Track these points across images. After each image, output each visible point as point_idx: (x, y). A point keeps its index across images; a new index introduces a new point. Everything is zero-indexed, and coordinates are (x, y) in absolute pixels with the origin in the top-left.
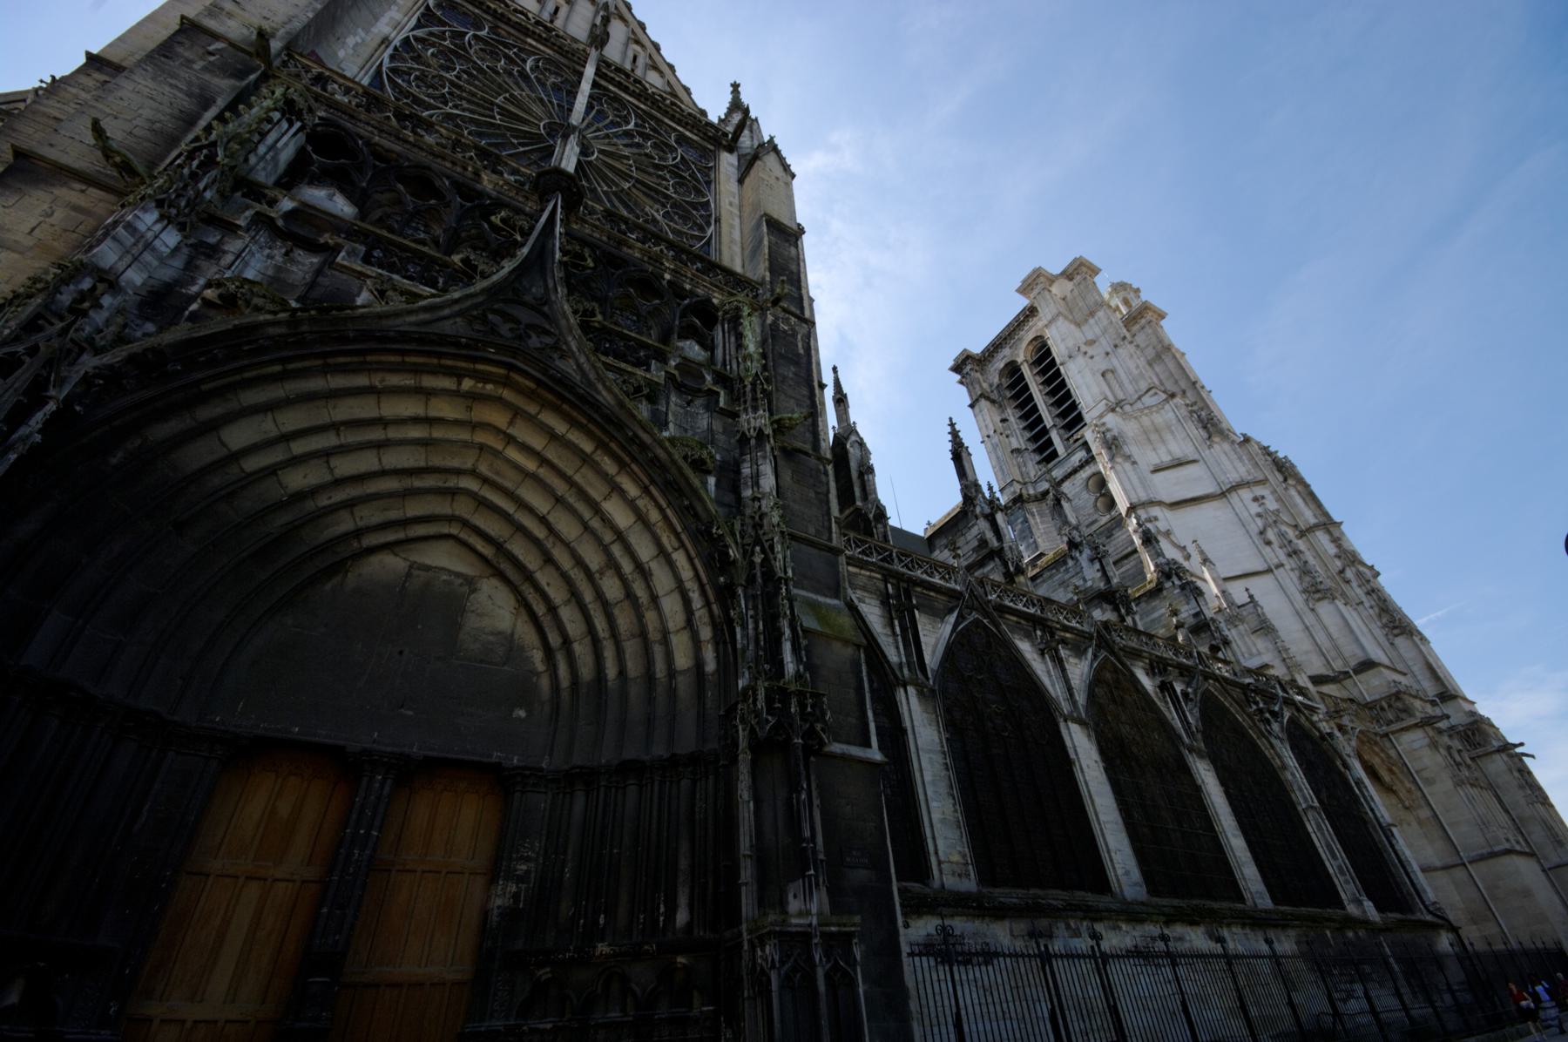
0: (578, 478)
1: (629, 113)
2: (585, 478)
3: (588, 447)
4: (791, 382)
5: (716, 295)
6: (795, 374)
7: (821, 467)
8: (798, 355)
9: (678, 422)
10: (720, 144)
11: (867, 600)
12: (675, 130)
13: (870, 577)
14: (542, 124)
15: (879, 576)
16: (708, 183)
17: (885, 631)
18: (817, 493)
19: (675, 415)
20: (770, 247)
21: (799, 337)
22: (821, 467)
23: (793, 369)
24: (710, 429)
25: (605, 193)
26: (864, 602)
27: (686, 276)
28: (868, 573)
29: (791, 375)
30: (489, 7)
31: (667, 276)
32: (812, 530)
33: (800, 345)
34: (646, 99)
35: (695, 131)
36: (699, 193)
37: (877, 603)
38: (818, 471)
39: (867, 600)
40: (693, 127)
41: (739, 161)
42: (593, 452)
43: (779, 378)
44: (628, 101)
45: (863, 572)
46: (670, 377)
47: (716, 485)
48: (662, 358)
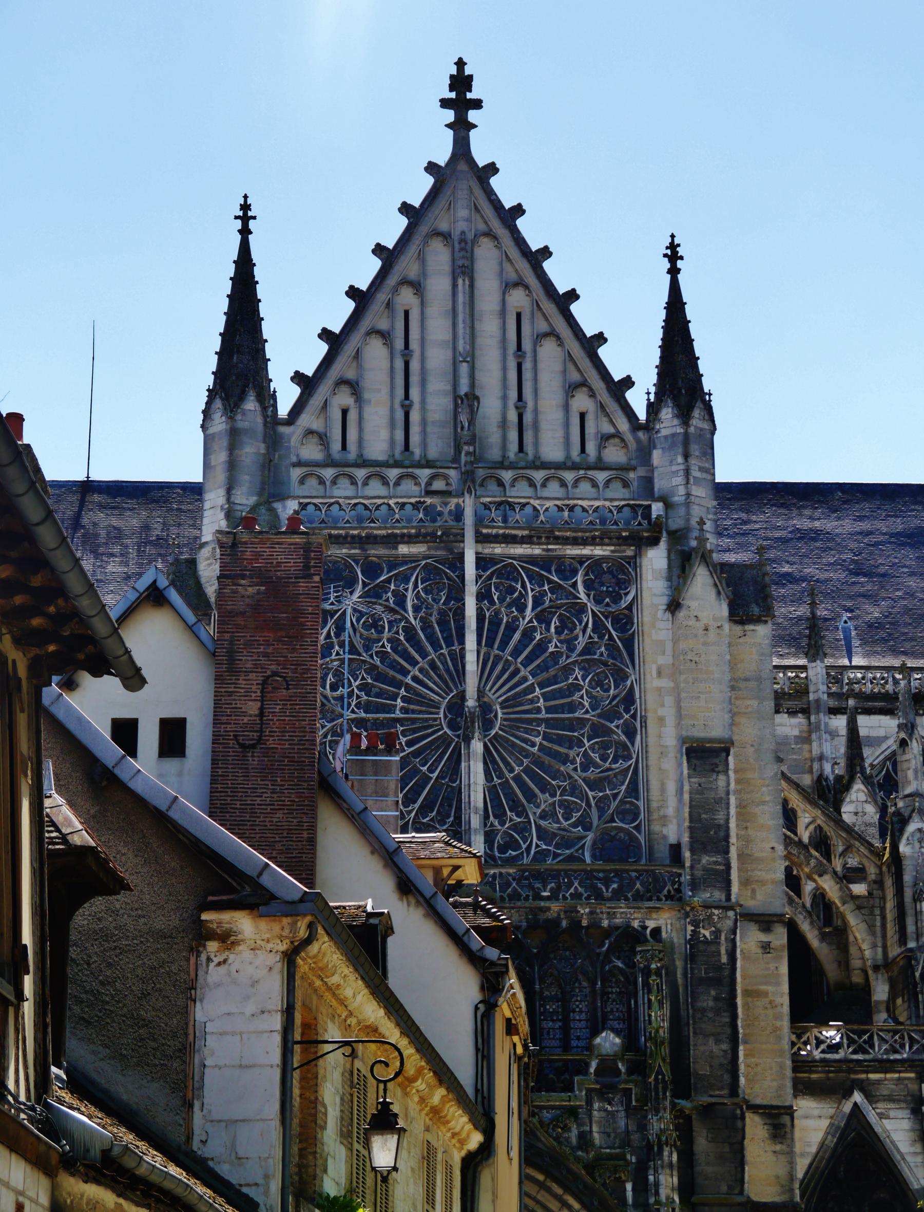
0: (539, 1197)
1: (524, 586)
2: (543, 1196)
3: (541, 1177)
4: (710, 1015)
5: (636, 915)
6: (716, 999)
7: (738, 1112)
8: (719, 968)
9: (602, 1129)
10: (641, 539)
11: (892, 1114)
12: (581, 560)
13: (899, 1079)
14: (442, 715)
15: (912, 1075)
16: (629, 644)
17: (912, 1150)
18: (731, 1144)
19: (599, 1123)
20: (691, 800)
21: (723, 938)
22: (738, 1112)
23: (713, 993)
24: (627, 1132)
25: (517, 778)
26: (888, 1118)
27: (602, 913)
28: (897, 1075)
29: (711, 1003)
30: (353, 537)
31: (585, 923)
32: (724, 1188)
33: (723, 951)
34: (539, 538)
35: (606, 541)
36: (620, 677)
37: (906, 1113)
38: (735, 1117)
39: (892, 1114)
40: (602, 539)
41: (669, 557)
42: (545, 1180)
43: (699, 1015)
44: (520, 558)
45: (888, 1076)
46: (589, 1091)
47: (633, 1190)
48: (582, 1068)
